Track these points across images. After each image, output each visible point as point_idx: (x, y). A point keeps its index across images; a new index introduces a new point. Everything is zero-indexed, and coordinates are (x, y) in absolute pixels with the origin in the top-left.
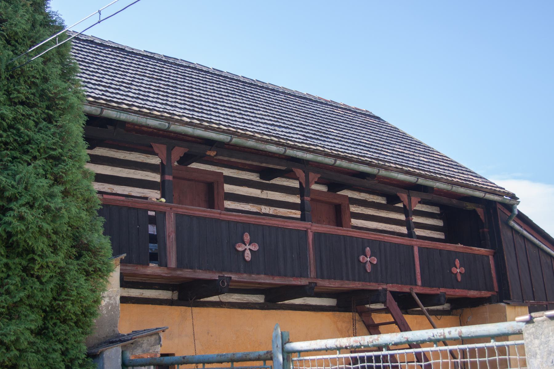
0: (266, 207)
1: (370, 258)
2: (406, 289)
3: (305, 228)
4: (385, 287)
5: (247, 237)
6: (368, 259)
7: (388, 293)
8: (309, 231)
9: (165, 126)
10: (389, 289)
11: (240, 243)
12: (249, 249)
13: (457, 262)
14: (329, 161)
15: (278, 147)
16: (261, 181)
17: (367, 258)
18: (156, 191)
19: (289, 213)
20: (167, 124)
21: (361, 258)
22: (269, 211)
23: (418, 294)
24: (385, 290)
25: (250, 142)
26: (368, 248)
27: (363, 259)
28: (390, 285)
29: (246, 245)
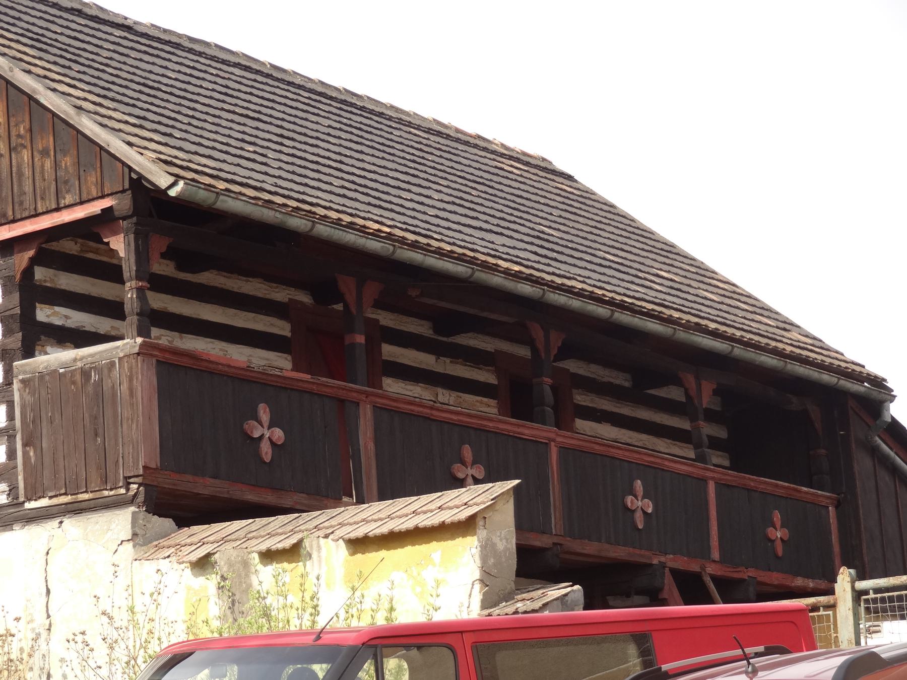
0: (445, 391)
1: (641, 501)
2: (695, 567)
3: (545, 438)
4: (663, 559)
5: (467, 453)
6: (640, 503)
7: (667, 570)
8: (553, 444)
9: (389, 250)
10: (671, 564)
11: (459, 465)
12: (472, 476)
13: (777, 517)
14: (602, 311)
15: (533, 286)
16: (436, 337)
17: (638, 500)
18: (286, 355)
19: (478, 404)
20: (391, 248)
21: (629, 499)
22: (449, 400)
23: (714, 578)
24: (663, 565)
25: (497, 277)
26: (639, 481)
27: (632, 502)
28: (671, 556)
29: (467, 468)
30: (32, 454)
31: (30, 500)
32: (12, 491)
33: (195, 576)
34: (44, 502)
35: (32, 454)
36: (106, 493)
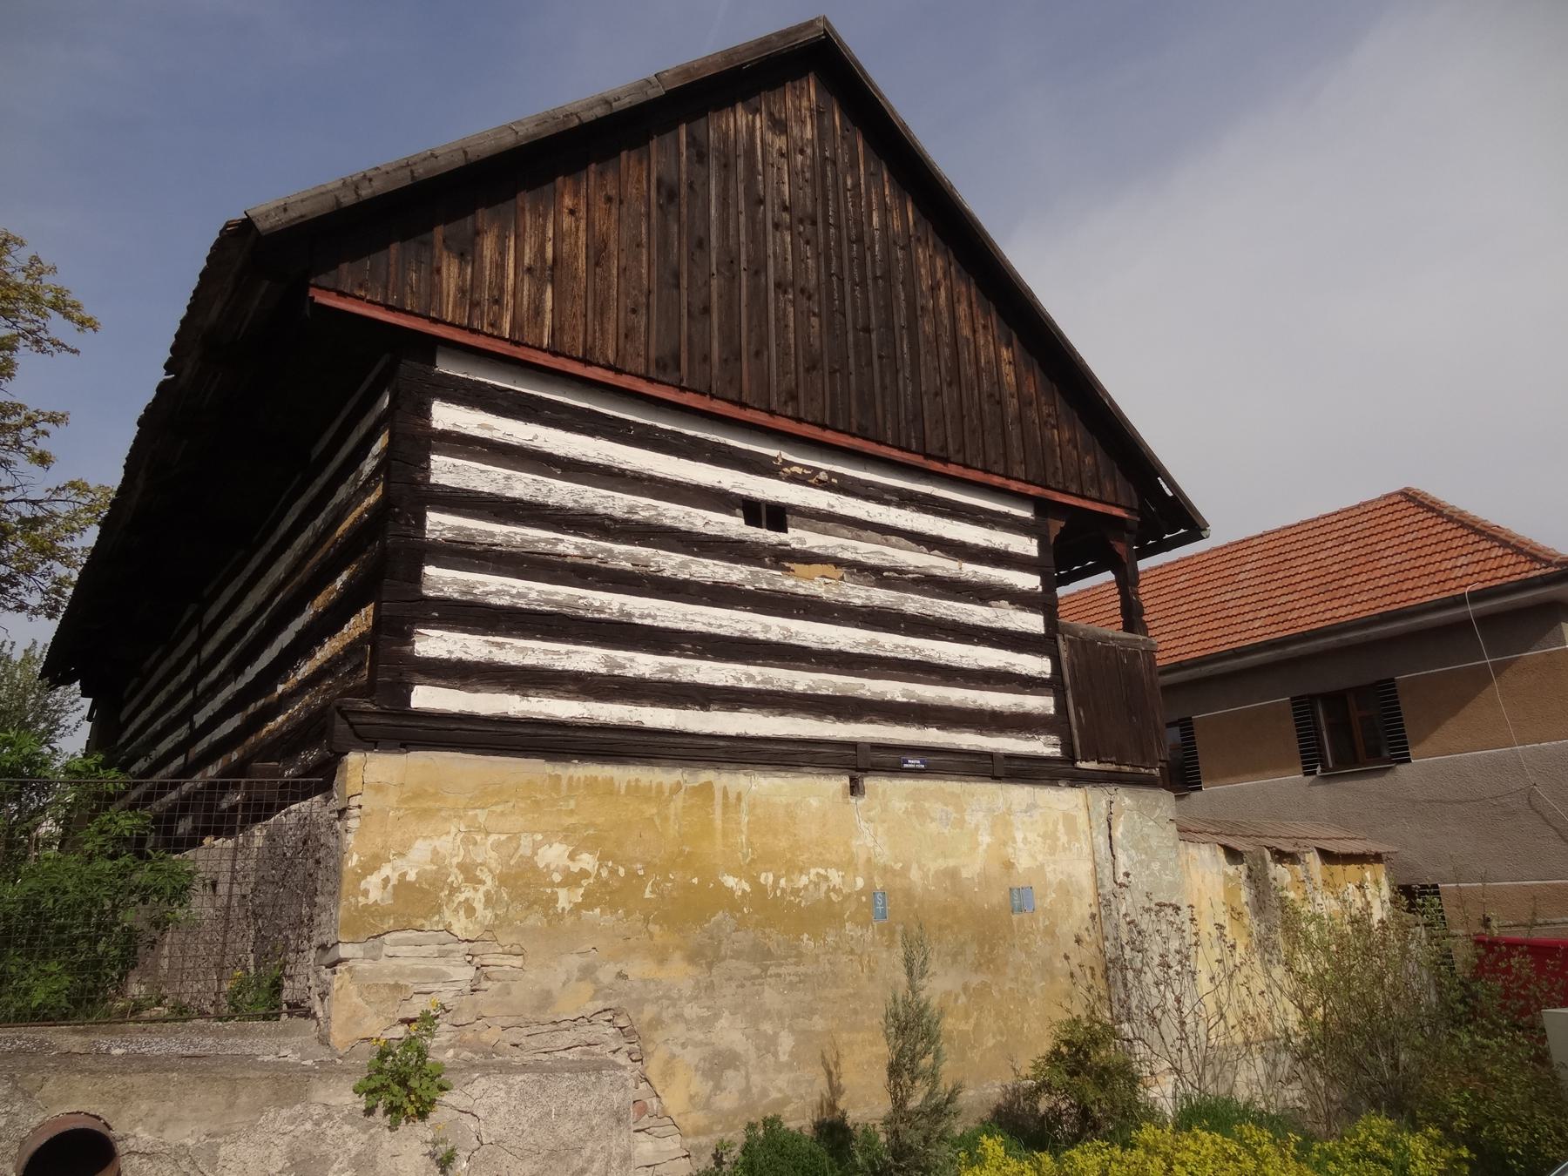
30: (1082, 714)
31: (1081, 761)
32: (1067, 746)
33: (1230, 864)
34: (1092, 765)
35: (1082, 714)
36: (1142, 770)
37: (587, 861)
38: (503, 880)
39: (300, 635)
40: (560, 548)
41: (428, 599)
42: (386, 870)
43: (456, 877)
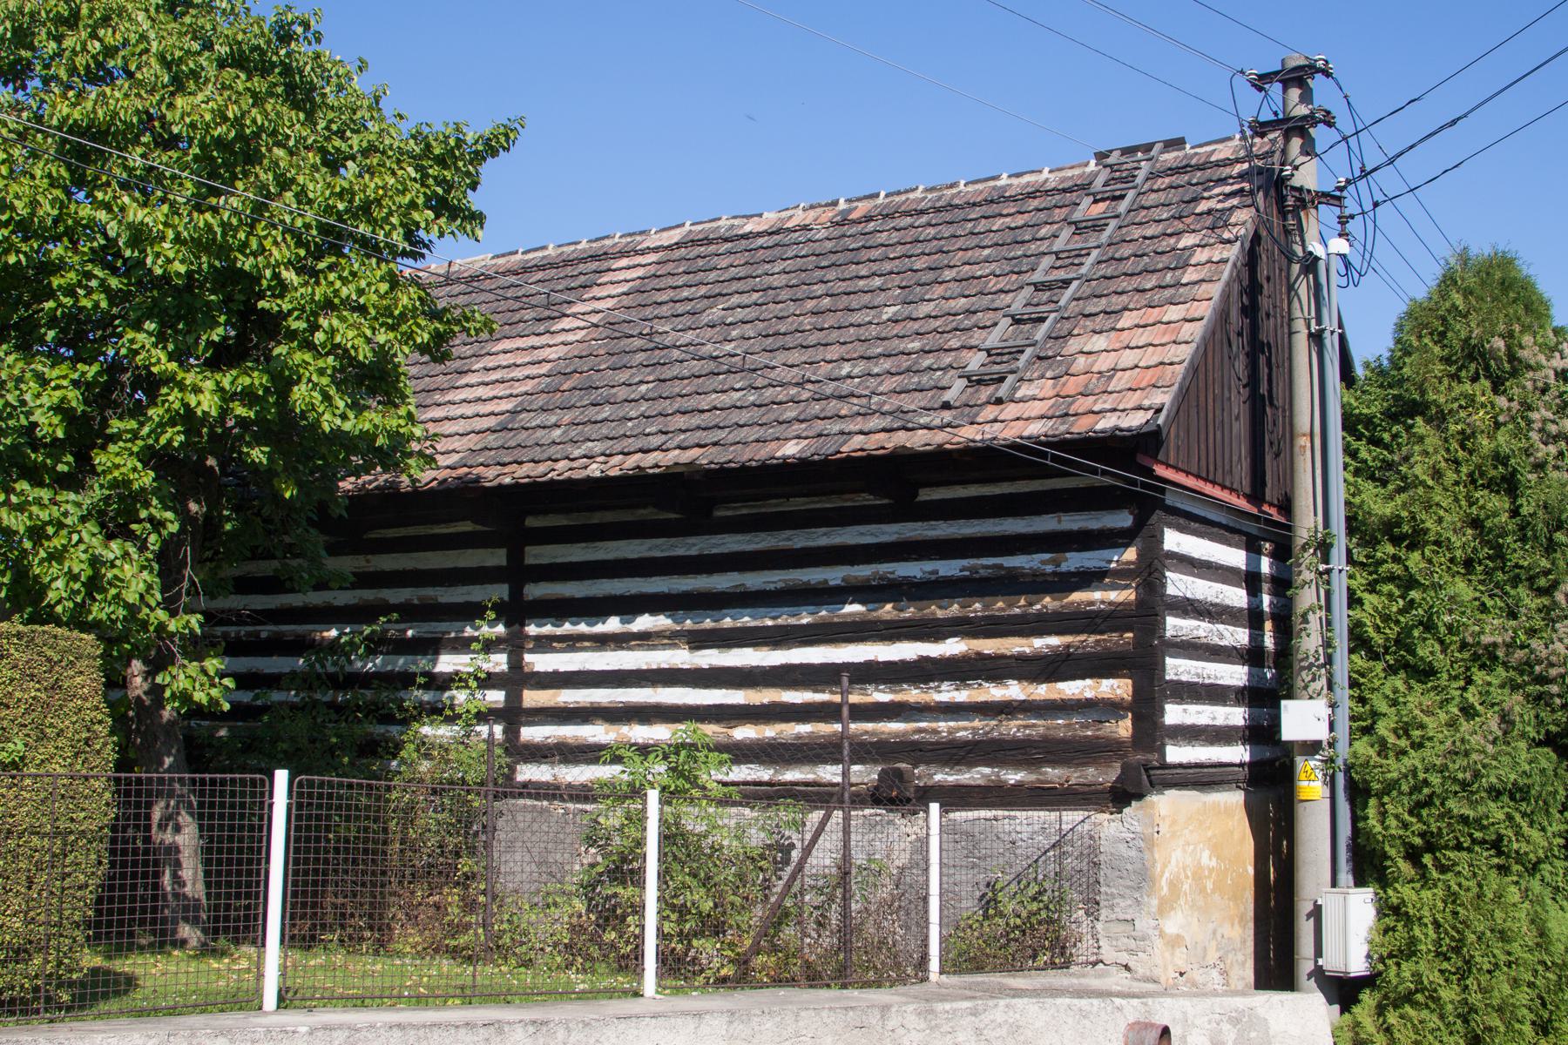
37: (1214, 863)
38: (1194, 874)
39: (924, 660)
40: (1201, 633)
41: (1168, 682)
42: (1167, 875)
43: (1182, 876)
